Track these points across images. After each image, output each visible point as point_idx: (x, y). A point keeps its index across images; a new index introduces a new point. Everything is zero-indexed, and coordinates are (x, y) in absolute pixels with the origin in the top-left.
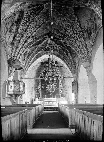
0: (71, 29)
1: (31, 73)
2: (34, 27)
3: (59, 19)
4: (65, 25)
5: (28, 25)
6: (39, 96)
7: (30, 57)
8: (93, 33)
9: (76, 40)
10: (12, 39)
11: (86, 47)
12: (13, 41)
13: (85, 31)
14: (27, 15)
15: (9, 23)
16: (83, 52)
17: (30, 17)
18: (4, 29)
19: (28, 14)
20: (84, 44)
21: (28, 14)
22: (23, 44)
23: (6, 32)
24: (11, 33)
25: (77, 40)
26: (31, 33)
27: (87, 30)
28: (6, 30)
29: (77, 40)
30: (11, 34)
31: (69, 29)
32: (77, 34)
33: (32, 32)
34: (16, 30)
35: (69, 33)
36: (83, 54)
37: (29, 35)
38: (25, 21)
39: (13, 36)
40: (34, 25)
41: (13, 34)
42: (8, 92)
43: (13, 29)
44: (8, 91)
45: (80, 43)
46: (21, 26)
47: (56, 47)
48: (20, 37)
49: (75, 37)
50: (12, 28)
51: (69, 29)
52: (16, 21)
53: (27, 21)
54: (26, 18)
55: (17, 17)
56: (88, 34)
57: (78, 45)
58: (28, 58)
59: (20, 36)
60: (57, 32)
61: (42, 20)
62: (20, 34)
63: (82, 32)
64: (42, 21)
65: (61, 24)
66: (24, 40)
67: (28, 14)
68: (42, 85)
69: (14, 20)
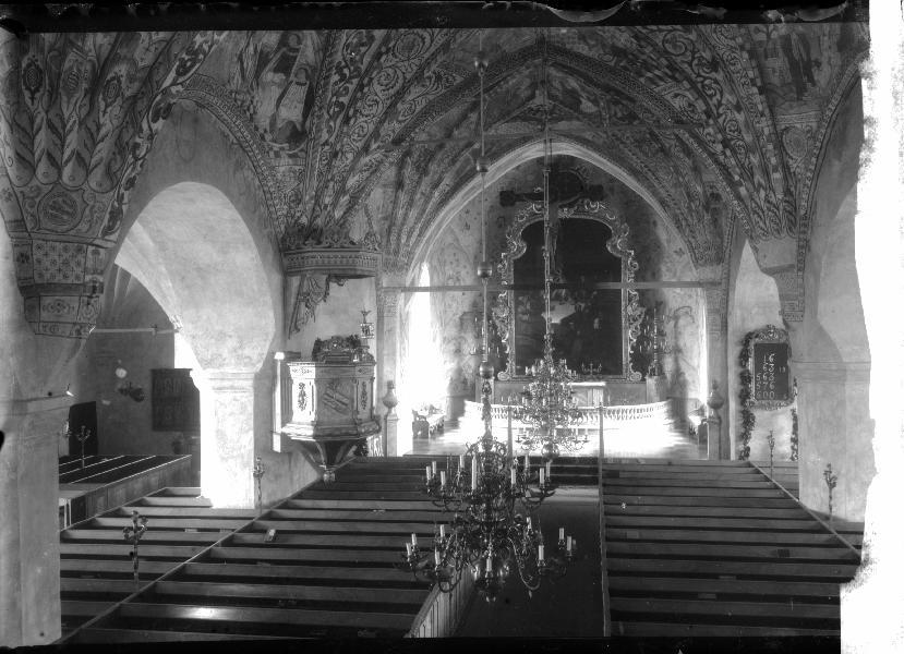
1: (452, 231)
6: (503, 368)
7: (433, 167)
8: (826, 68)
9: (711, 96)
11: (780, 147)
12: (305, 116)
13: (770, 46)
16: (758, 178)
18: (240, 59)
20: (764, 126)
22: (372, 127)
23: (257, 74)
25: (718, 96)
26: (417, 61)
27: (781, 37)
28: (250, 64)
29: (718, 96)
30: (292, 77)
32: (714, 65)
33: (426, 56)
34: (316, 52)
35: (667, 52)
36: (760, 185)
37: (408, 76)
39: (305, 89)
41: (303, 80)
42: (283, 425)
43: (297, 50)
44: (287, 417)
45: (740, 117)
47: (590, 104)
48: (346, 89)
49: (705, 78)
56: (794, 65)
57: (722, 130)
58: (422, 171)
59: (351, 87)
60: (588, 44)
62: (346, 71)
63: (753, 54)
66: (375, 108)
68: (518, 304)
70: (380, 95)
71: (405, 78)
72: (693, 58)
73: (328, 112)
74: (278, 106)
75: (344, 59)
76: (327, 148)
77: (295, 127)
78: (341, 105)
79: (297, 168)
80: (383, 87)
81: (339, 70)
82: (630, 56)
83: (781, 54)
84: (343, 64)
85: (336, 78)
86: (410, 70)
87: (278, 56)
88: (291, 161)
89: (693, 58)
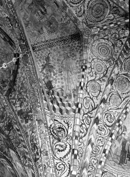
0: (92, 100)
3: (98, 59)
4: (93, 78)
29: (83, 135)
31: (88, 94)
49: (84, 124)
51: (88, 94)
61: (81, 9)
64: (78, 10)
65: (91, 67)
72: (86, 114)
82: (51, 91)
83: (121, 142)
89: (86, 114)
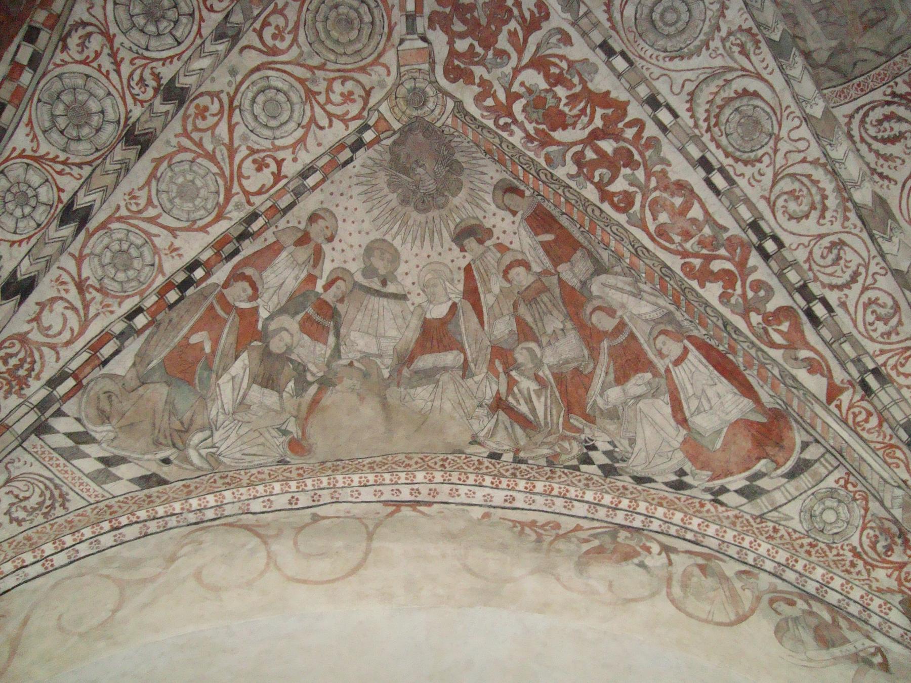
2: (718, 62)
5: (646, 134)
10: (724, 386)
12: (747, 390)
14: (517, 107)
15: (525, 332)
17: (570, 86)
19: (513, 97)
21: (516, 88)
24: (649, 366)
26: (787, 125)
30: (661, 365)
34: (638, 294)
38: (598, 150)
39: (694, 355)
40: (695, 62)
41: (674, 349)
43: (622, 325)
46: (622, 218)
48: (758, 285)
50: (605, 323)
52: (545, 246)
53: (598, 123)
54: (559, 121)
55: (509, 217)
66: (848, 255)
67: (513, 97)
69: (527, 265)
70: (823, 230)
71: (815, 163)
73: (773, 345)
74: (683, 421)
75: (685, 254)
76: (845, 398)
77: (749, 424)
78: (784, 312)
79: (830, 482)
80: (815, 215)
81: (705, 276)
84: (697, 262)
85: (712, 292)
86: (802, 145)
87: (604, 359)
88: (805, 480)
